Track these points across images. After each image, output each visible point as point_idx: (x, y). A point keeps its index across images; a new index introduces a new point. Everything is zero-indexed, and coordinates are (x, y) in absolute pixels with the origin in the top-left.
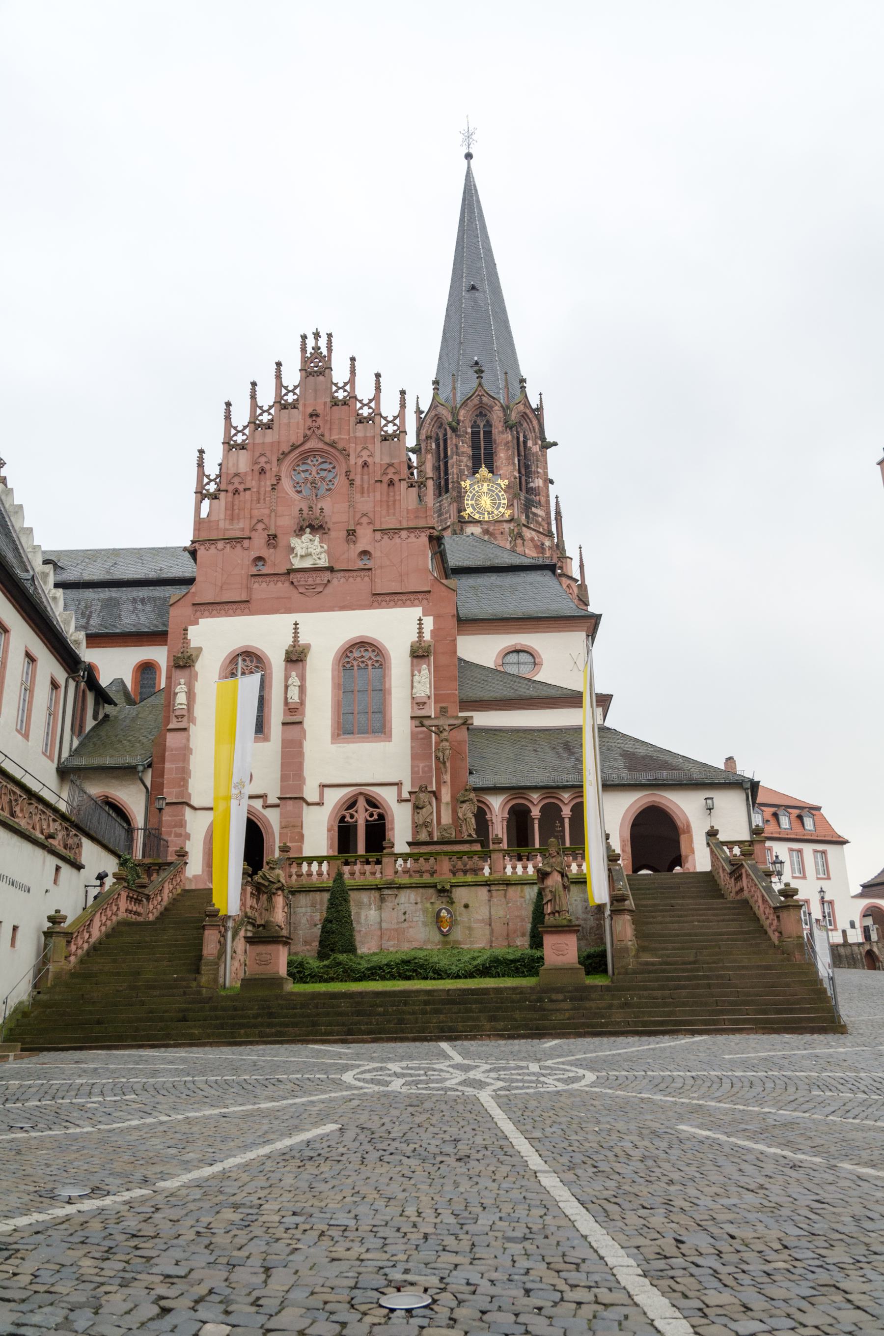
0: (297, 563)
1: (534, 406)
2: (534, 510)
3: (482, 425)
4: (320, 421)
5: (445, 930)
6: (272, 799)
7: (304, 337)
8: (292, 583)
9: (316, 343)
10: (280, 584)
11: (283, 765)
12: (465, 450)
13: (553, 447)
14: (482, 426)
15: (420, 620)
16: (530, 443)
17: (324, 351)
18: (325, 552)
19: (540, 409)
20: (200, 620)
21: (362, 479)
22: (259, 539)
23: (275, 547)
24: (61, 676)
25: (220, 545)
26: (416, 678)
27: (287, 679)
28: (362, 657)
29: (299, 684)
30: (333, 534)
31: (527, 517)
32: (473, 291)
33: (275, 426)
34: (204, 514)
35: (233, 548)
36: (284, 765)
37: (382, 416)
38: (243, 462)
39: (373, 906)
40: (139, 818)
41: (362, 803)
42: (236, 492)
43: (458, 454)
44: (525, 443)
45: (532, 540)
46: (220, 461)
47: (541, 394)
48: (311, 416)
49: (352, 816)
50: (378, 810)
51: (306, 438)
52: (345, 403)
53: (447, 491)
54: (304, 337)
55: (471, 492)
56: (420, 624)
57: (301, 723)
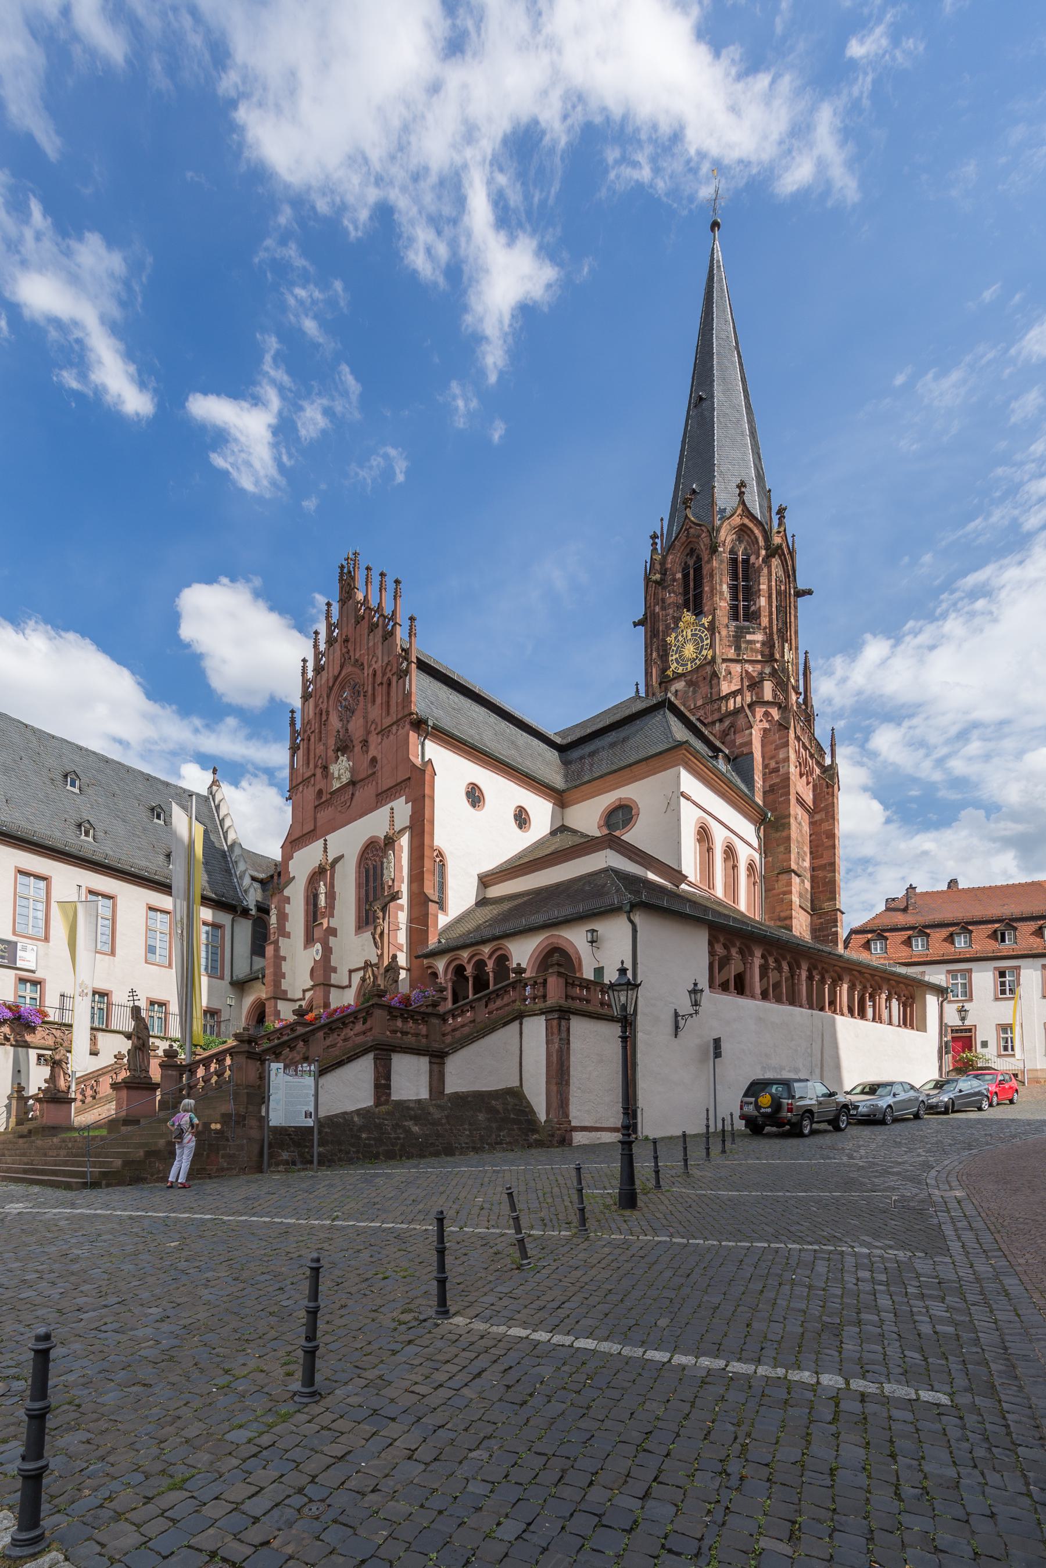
0: (336, 785)
2: (749, 637)
22: (319, 771)
28: (374, 855)
31: (738, 648)
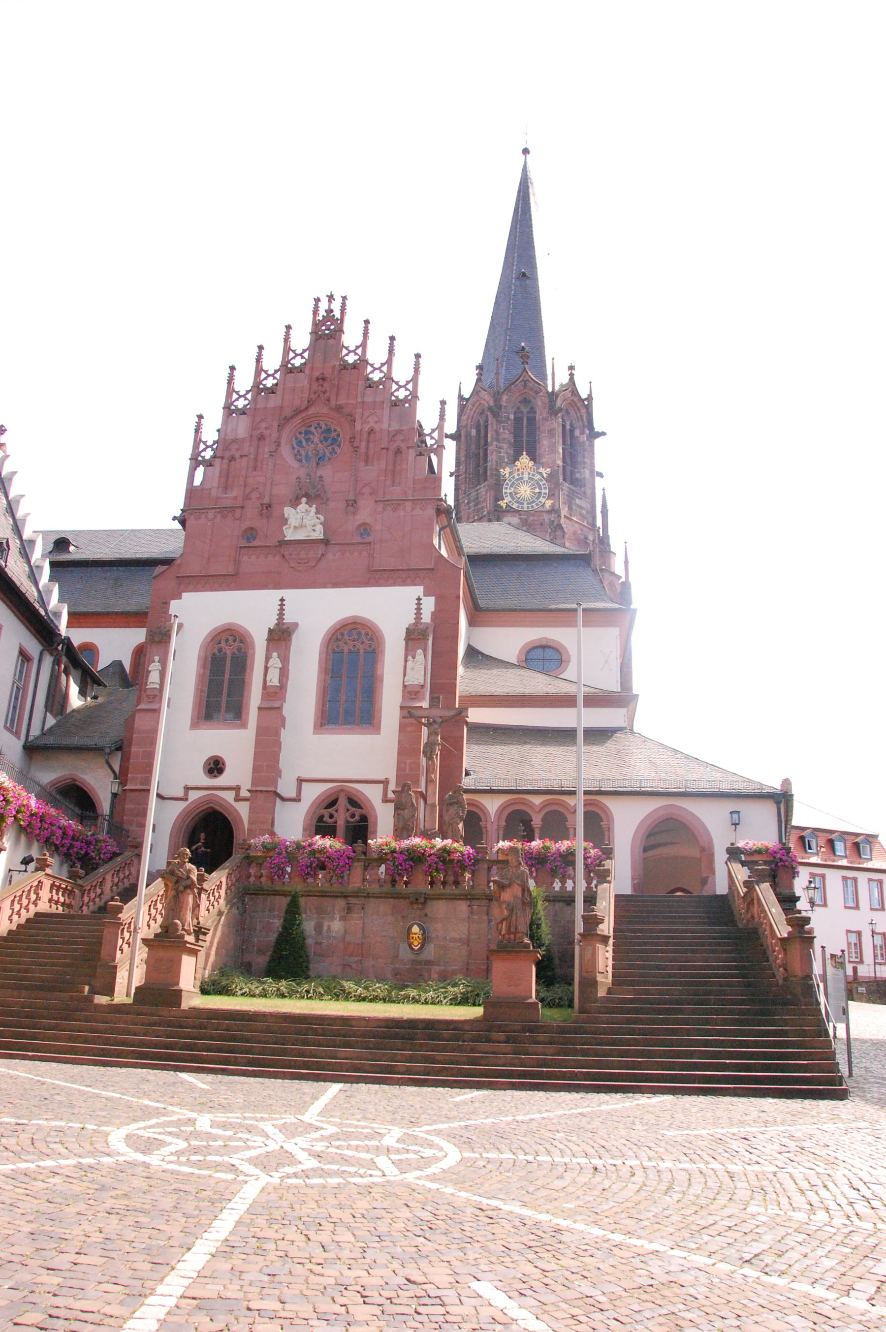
1: (584, 396)
3: (525, 410)
4: (326, 385)
5: (416, 948)
6: (244, 793)
7: (317, 300)
8: (283, 555)
9: (329, 306)
10: (270, 558)
11: (256, 754)
12: (506, 436)
13: (602, 438)
14: (525, 413)
15: (419, 599)
16: (577, 433)
17: (337, 314)
18: (321, 524)
19: (590, 398)
20: (184, 594)
21: (367, 448)
22: (252, 510)
23: (268, 517)
24: (34, 647)
25: (211, 515)
26: (409, 664)
27: (268, 658)
29: (280, 666)
30: (332, 505)
31: (570, 508)
32: (524, 278)
33: (279, 391)
34: (197, 481)
35: (224, 517)
36: (258, 755)
37: (393, 381)
38: (242, 427)
39: (337, 916)
40: (105, 805)
41: (342, 803)
42: (232, 459)
43: (497, 440)
44: (572, 431)
45: (575, 533)
46: (219, 427)
47: (590, 383)
48: (318, 379)
49: (331, 816)
50: (360, 810)
51: (311, 403)
52: (354, 366)
53: (486, 480)
54: (317, 300)
55: (510, 480)
56: (419, 604)
57: (279, 709)
